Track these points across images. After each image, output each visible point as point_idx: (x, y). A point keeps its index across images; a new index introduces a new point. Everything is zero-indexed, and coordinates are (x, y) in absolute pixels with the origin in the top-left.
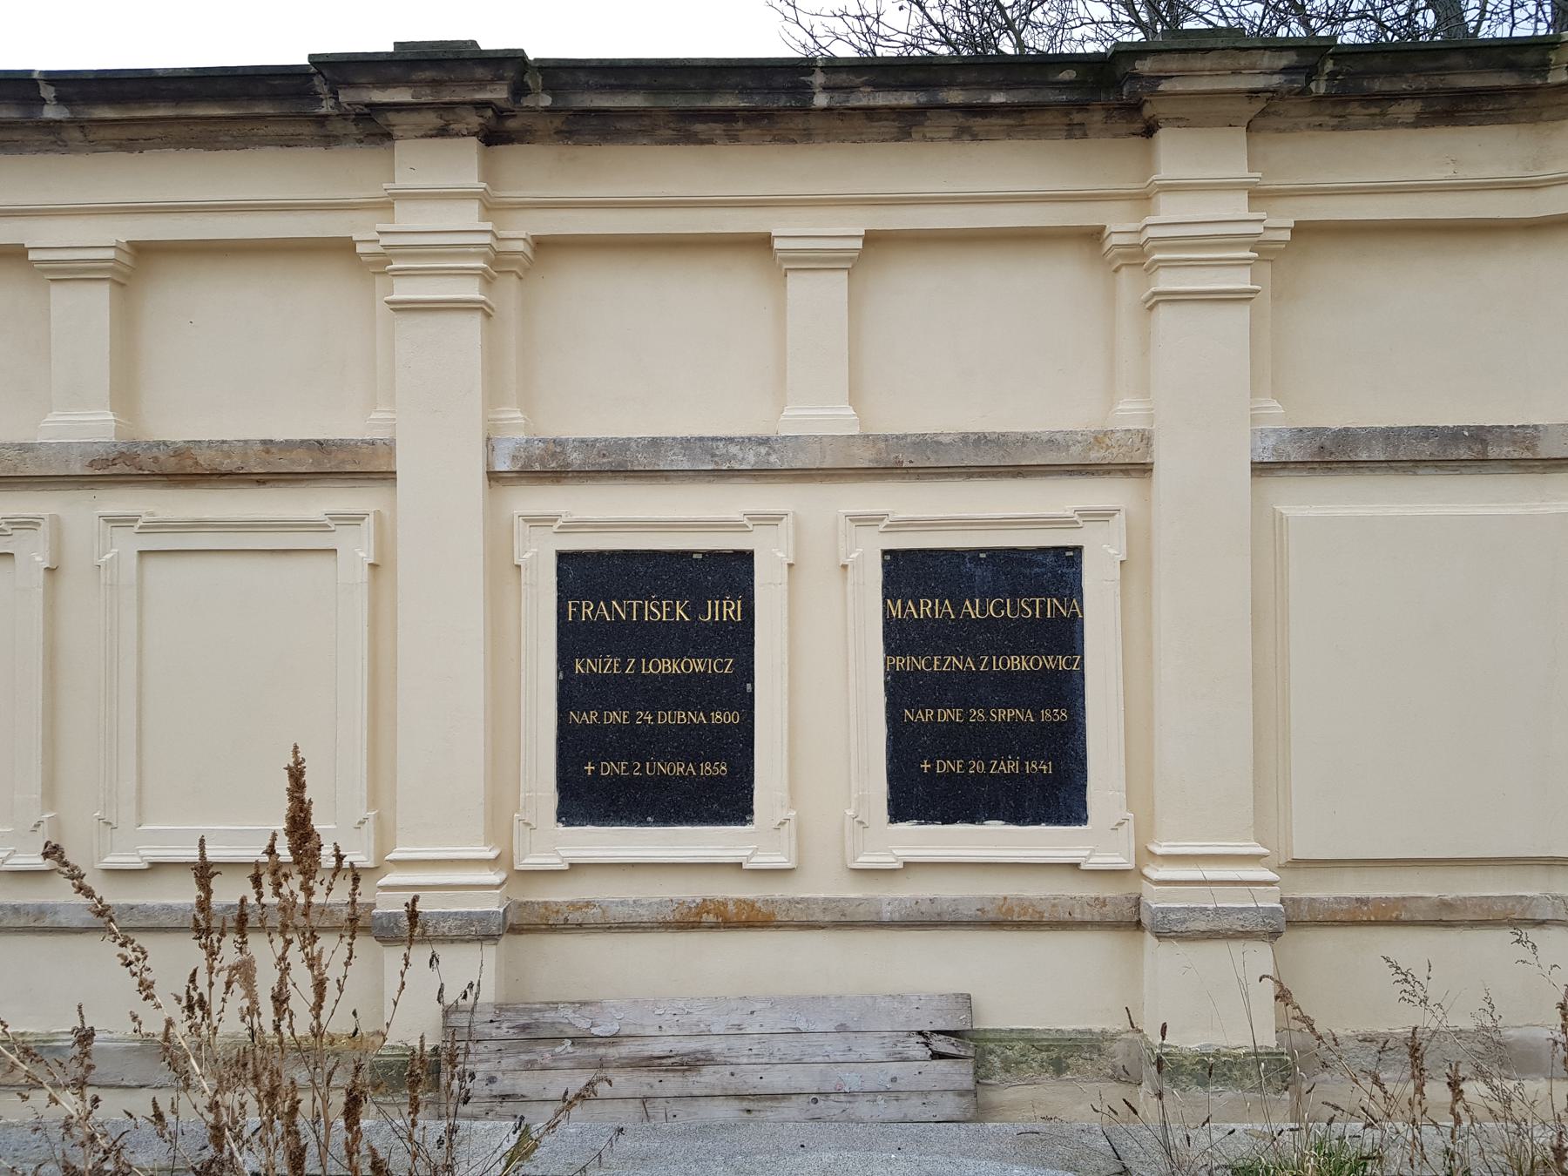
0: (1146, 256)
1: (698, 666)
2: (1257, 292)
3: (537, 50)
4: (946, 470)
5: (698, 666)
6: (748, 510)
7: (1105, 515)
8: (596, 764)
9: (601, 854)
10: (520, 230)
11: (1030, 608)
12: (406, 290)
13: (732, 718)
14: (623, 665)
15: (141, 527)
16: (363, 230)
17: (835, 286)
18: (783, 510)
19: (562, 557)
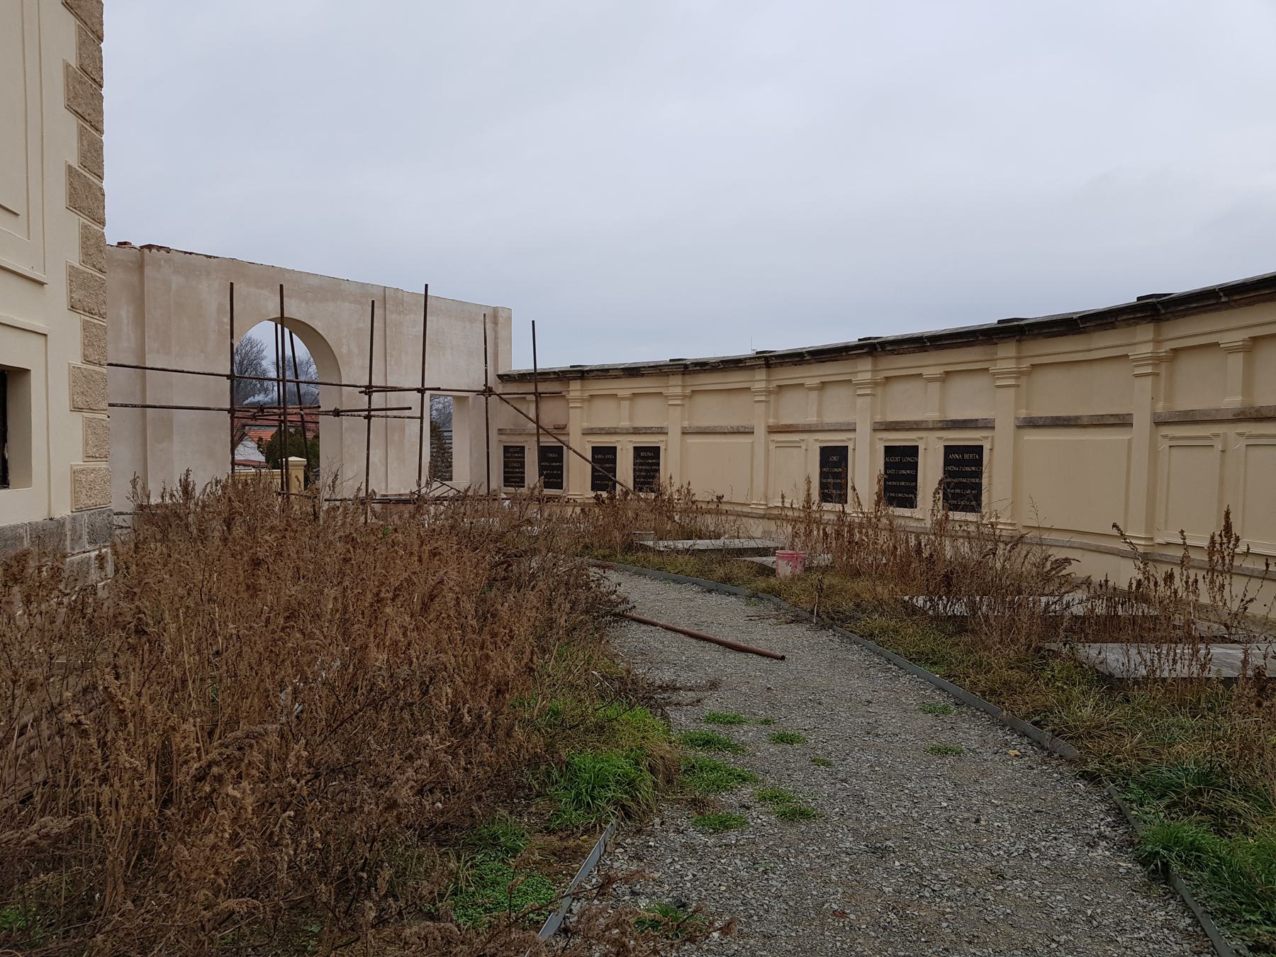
17: (937, 385)
19: (885, 447)
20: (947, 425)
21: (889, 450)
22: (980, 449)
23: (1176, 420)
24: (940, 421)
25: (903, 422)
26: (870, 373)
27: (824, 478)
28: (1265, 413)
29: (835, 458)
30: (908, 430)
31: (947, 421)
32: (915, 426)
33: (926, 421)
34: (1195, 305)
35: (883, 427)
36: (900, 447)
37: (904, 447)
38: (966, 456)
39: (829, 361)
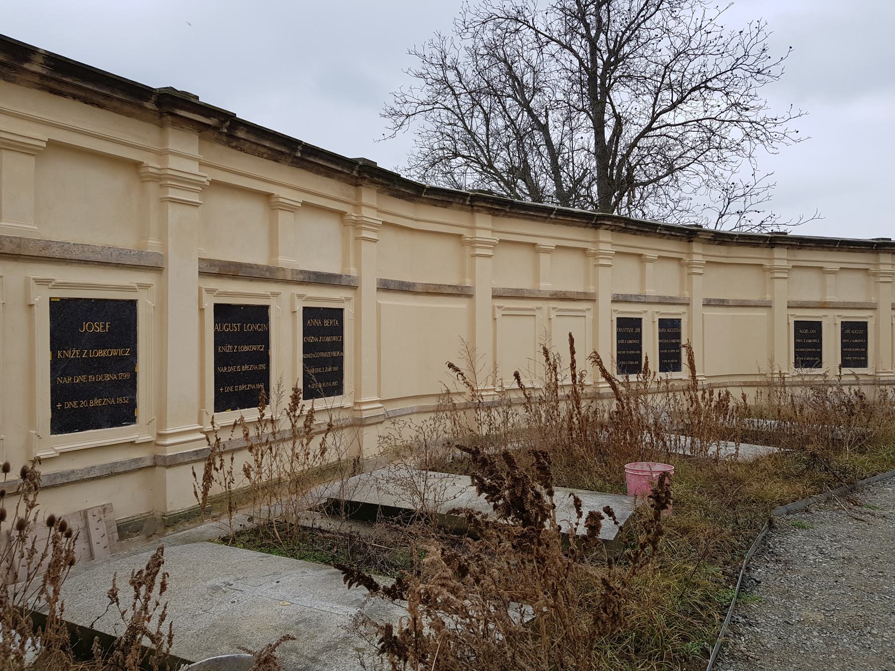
0: (357, 224)
1: (254, 348)
2: (378, 240)
3: (239, 116)
4: (29, 257)
5: (254, 348)
6: (272, 291)
7: (348, 299)
8: (224, 388)
9: (143, 438)
10: (210, 175)
11: (250, 327)
12: (173, 194)
13: (263, 366)
14: (233, 349)
15: (54, 285)
16: (152, 163)
18: (279, 292)
20: (309, 278)
21: (220, 309)
22: (338, 313)
23: (509, 295)
24: (302, 272)
25: (250, 266)
26: (45, 143)
27: (64, 374)
28: (569, 296)
29: (99, 328)
30: (252, 278)
31: (309, 272)
32: (267, 275)
33: (283, 269)
34: (532, 213)
35: (216, 271)
36: (240, 306)
37: (246, 306)
38: (326, 323)
39: (75, 97)
